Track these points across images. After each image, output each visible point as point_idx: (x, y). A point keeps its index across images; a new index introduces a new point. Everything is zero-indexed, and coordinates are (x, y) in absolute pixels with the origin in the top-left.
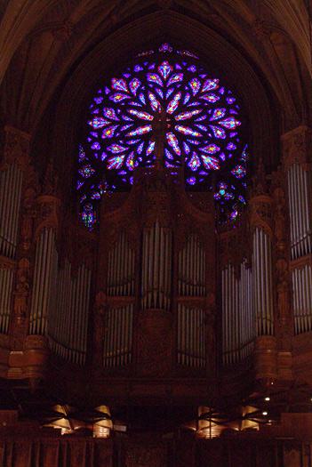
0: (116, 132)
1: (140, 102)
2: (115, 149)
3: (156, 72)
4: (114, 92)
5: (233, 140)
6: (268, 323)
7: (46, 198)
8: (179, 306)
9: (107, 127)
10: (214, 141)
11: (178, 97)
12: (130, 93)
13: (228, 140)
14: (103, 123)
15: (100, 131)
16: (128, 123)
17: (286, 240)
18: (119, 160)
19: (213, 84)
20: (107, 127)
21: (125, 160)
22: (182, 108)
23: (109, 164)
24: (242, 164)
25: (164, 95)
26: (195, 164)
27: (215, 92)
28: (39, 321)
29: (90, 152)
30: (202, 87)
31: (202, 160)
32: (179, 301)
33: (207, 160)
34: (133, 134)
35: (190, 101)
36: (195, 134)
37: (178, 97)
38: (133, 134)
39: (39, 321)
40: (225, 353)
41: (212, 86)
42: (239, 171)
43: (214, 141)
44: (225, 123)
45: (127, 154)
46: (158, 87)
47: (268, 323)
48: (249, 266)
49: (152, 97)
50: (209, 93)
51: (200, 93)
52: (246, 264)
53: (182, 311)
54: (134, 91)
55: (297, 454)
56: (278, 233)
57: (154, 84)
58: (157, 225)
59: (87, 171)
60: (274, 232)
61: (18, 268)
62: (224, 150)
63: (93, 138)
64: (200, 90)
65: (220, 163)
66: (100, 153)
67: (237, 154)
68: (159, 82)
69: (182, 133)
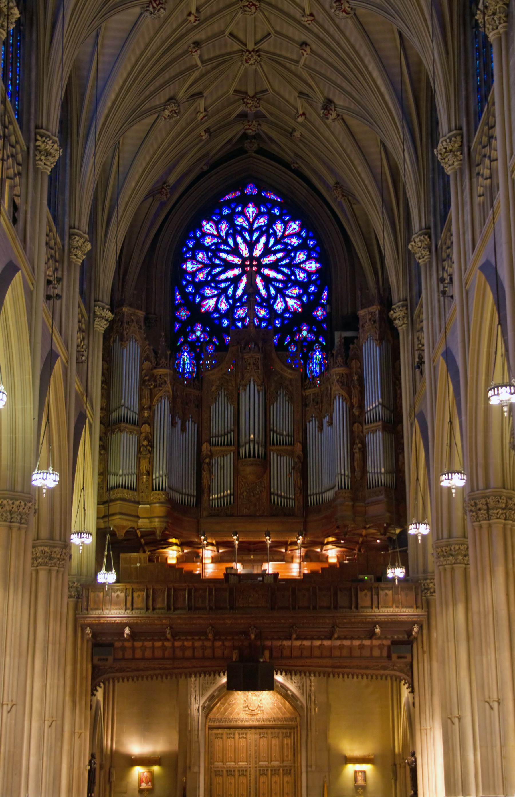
0: (207, 275)
1: (228, 245)
2: (208, 292)
3: (242, 214)
4: (204, 235)
5: (314, 283)
6: (346, 478)
7: (161, 371)
8: (272, 454)
9: (199, 270)
10: (297, 283)
11: (263, 240)
12: (219, 236)
13: (310, 282)
14: (196, 266)
15: (194, 274)
16: (218, 266)
17: (362, 406)
18: (211, 303)
19: (295, 226)
20: (199, 270)
21: (217, 303)
22: (267, 251)
23: (203, 306)
24: (323, 306)
25: (251, 238)
26: (279, 306)
27: (298, 235)
28: (161, 479)
29: (185, 295)
30: (285, 230)
31: (286, 302)
32: (272, 450)
33: (291, 302)
34: (223, 277)
35: (275, 244)
36: (280, 277)
37: (263, 240)
38: (223, 277)
39: (161, 479)
40: (311, 495)
41: (294, 229)
42: (320, 313)
43: (297, 283)
44: (307, 266)
45: (218, 296)
46: (245, 229)
47: (346, 478)
48: (330, 423)
49: (239, 240)
50: (291, 236)
51: (283, 236)
52: (328, 422)
53: (274, 457)
54: (223, 234)
55: (369, 594)
56: (355, 400)
57: (241, 226)
58: (252, 383)
59: (183, 313)
60: (351, 399)
61: (141, 433)
62: (306, 292)
63: (187, 281)
64: (284, 232)
65: (303, 305)
66: (194, 295)
67: (318, 295)
68: (246, 225)
69: (268, 276)
